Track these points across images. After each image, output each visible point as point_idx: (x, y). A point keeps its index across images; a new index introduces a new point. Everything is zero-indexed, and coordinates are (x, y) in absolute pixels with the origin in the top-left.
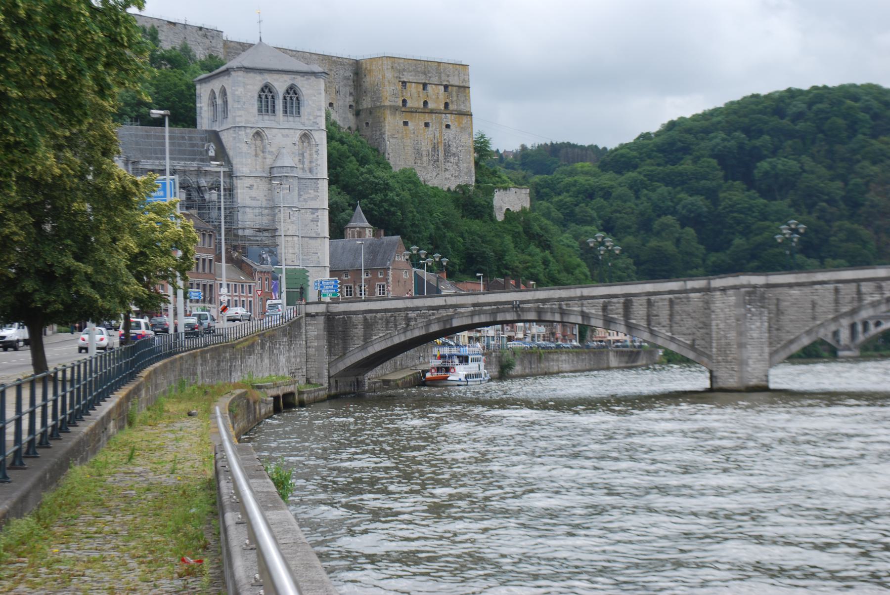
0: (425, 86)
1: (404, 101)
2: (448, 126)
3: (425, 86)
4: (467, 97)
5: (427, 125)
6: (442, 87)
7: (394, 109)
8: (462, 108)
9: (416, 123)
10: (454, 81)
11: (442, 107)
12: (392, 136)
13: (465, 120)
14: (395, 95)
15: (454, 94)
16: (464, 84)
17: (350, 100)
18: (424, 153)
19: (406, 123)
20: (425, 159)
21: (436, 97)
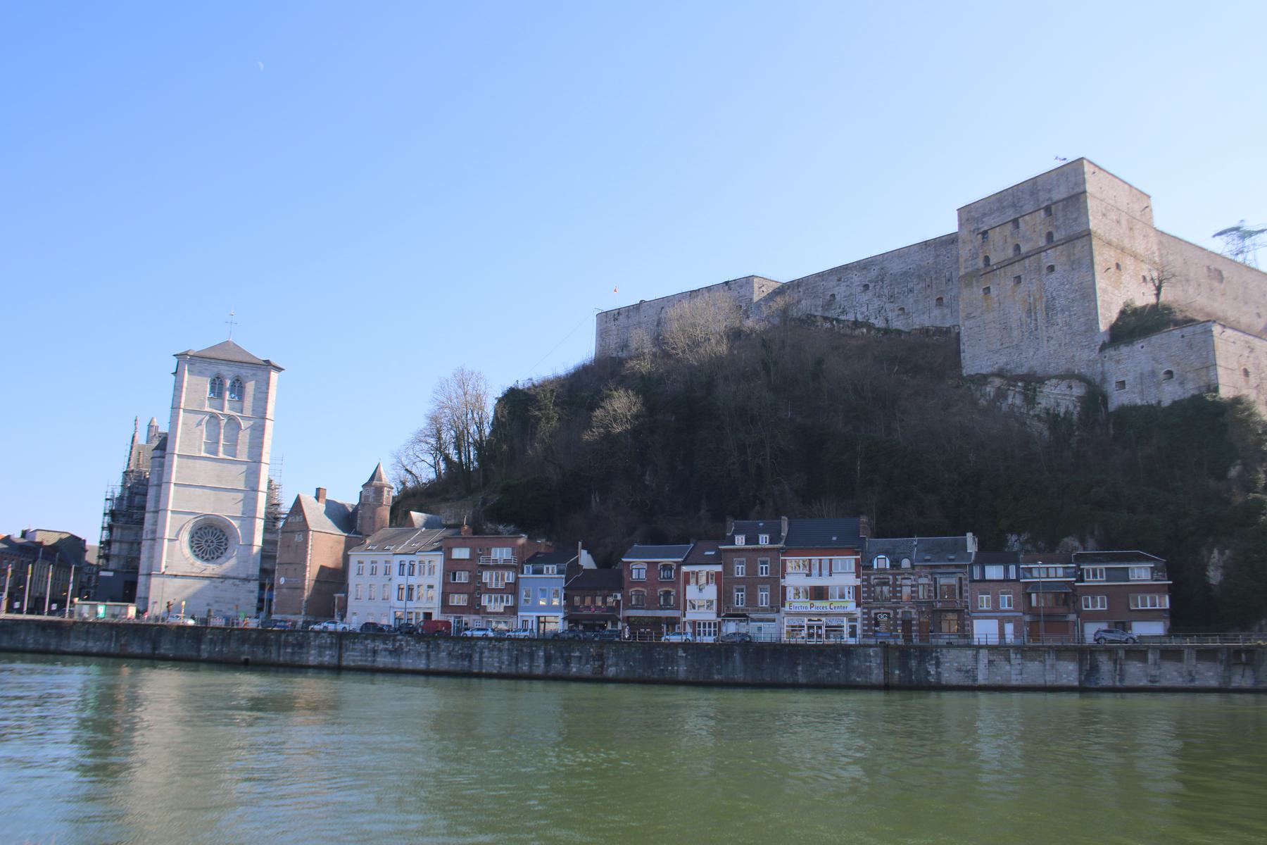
3: (1015, 222)
4: (1084, 210)
5: (1018, 279)
6: (1042, 212)
8: (1077, 229)
9: (1002, 285)
10: (1060, 193)
11: (1042, 242)
13: (1079, 244)
14: (974, 256)
16: (1077, 190)
19: (987, 290)
20: (1015, 333)
21: (1034, 229)
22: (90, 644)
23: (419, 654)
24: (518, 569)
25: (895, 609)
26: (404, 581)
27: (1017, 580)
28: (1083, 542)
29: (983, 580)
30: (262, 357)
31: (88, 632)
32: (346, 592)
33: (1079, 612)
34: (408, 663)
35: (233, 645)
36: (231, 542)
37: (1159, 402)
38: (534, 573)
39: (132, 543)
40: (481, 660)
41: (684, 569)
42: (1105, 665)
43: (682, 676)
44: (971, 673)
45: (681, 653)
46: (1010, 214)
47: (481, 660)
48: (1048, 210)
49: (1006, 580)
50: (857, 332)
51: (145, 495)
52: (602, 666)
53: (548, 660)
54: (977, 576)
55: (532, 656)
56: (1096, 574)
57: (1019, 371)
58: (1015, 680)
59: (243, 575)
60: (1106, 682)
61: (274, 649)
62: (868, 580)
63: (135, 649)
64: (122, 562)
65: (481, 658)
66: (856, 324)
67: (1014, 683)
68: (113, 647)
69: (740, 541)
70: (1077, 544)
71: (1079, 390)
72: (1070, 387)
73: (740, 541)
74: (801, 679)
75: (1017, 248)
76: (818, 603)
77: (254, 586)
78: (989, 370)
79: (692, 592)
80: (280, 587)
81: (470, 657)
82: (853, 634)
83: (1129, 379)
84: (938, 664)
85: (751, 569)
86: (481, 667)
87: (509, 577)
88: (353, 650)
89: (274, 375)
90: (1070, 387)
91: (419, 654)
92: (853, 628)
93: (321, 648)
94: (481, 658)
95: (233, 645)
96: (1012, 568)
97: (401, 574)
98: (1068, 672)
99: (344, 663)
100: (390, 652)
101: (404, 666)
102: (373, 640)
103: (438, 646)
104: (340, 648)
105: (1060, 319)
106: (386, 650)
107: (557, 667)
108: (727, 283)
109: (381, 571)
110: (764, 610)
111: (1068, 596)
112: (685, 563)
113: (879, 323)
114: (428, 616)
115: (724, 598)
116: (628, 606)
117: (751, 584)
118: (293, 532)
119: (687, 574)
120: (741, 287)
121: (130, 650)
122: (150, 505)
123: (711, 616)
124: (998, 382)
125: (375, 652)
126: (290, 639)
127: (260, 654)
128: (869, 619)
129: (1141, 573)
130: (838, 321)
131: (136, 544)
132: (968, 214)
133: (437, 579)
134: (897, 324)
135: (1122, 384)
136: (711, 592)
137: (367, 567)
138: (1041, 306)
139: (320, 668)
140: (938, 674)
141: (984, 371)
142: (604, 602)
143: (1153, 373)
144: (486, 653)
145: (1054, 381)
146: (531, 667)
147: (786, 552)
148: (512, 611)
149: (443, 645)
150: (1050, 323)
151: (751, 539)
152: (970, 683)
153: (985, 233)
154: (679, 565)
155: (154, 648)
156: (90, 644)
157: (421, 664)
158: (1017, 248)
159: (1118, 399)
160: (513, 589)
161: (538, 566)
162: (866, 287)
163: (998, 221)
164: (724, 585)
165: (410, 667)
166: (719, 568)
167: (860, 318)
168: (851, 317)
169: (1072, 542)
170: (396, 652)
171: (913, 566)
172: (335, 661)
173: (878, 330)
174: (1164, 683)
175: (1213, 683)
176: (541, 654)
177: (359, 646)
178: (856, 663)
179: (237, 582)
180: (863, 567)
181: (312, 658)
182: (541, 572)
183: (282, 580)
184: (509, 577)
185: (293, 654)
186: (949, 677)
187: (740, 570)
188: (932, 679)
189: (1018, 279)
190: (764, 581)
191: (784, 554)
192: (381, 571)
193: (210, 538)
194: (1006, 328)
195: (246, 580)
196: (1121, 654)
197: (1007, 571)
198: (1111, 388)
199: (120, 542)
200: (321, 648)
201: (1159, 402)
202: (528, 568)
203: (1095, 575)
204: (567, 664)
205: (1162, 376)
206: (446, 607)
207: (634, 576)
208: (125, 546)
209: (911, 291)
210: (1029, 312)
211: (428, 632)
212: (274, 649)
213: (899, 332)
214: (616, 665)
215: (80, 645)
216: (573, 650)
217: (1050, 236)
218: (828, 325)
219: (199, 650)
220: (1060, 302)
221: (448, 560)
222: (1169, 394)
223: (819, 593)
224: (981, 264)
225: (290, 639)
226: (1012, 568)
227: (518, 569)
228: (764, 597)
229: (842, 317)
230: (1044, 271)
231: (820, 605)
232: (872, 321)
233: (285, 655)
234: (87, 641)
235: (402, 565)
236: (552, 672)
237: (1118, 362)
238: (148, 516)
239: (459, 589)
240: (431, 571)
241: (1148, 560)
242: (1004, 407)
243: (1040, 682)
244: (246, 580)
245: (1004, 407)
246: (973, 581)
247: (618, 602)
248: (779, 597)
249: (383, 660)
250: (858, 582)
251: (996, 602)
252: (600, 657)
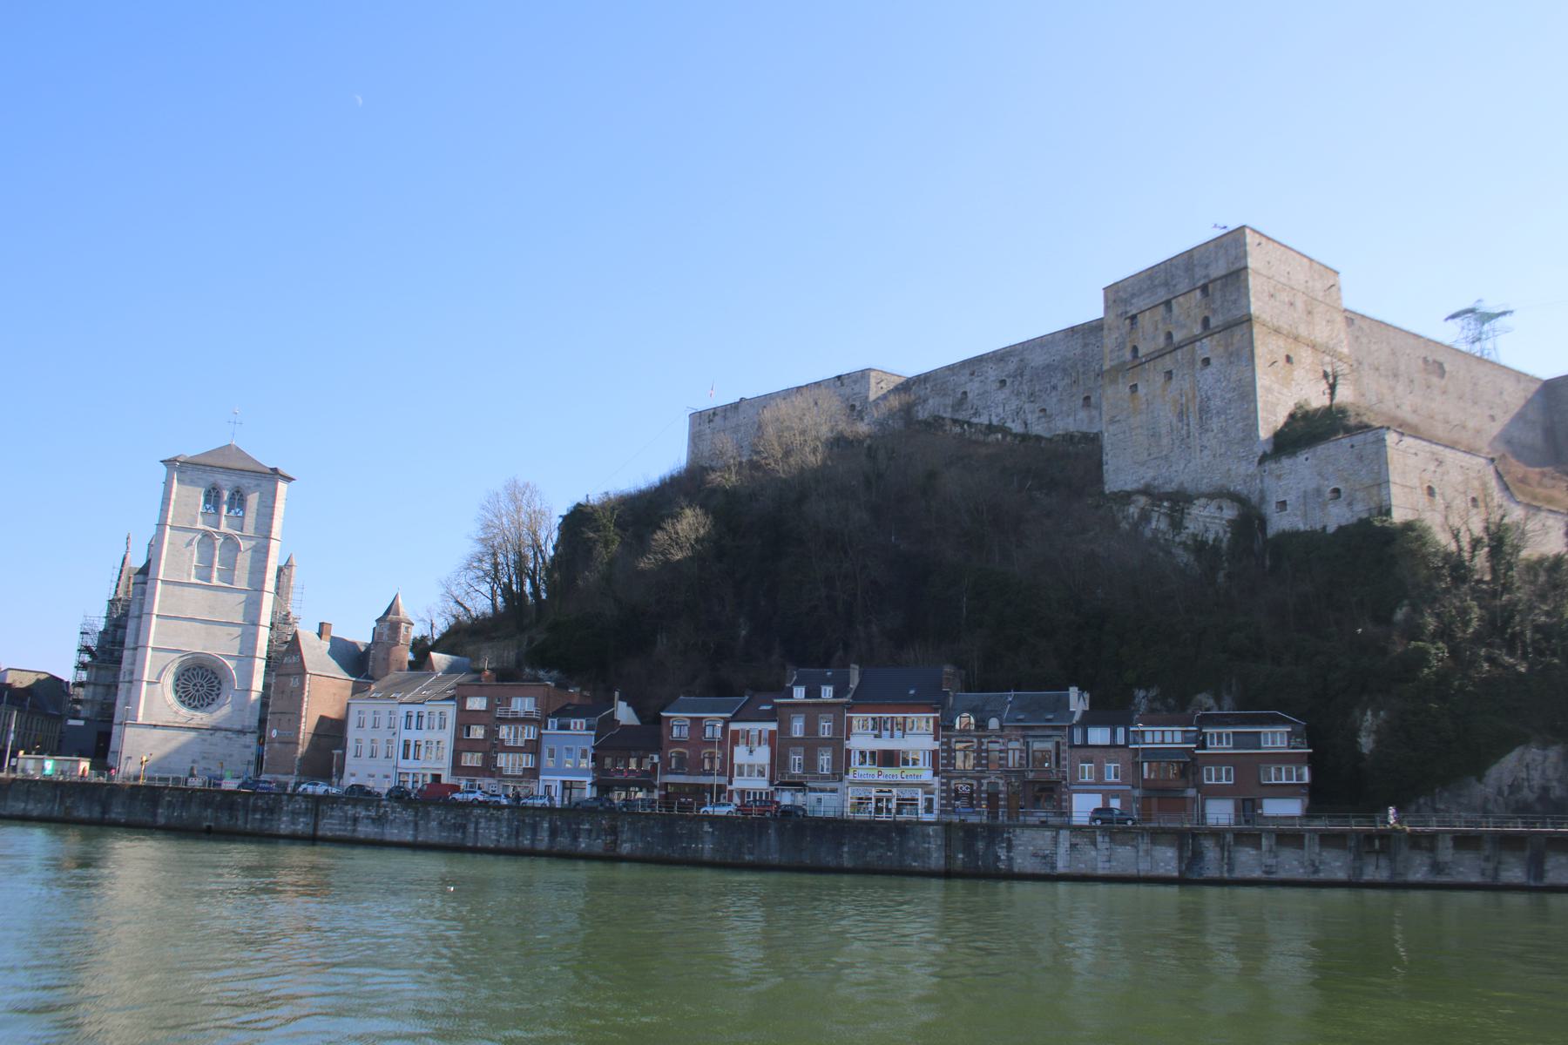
3: (1168, 303)
4: (1243, 290)
5: (1169, 375)
6: (1198, 292)
9: (1151, 383)
10: (1218, 270)
11: (1197, 329)
13: (1238, 333)
14: (1121, 346)
15: (1218, 295)
16: (1237, 266)
18: (1164, 431)
19: (1134, 388)
20: (1165, 441)
22: (30, 807)
23: (406, 823)
24: (541, 723)
25: (979, 779)
27: (1126, 746)
28: (1218, 699)
29: (1085, 745)
30: (270, 464)
31: (28, 793)
32: (344, 749)
33: (1199, 786)
34: (392, 833)
35: (194, 810)
36: (225, 686)
37: (1324, 528)
38: (561, 727)
39: (109, 686)
40: (476, 833)
41: (733, 726)
42: (1211, 852)
43: (707, 856)
44: (1049, 859)
45: (707, 828)
46: (1162, 295)
47: (476, 833)
48: (1204, 289)
49: (1113, 746)
50: (992, 438)
51: (125, 628)
52: (615, 842)
53: (553, 833)
54: (1078, 740)
55: (534, 828)
56: (1220, 740)
57: (1168, 488)
58: (1102, 869)
59: (238, 727)
60: (1212, 872)
61: (241, 815)
62: (948, 743)
63: (82, 813)
64: (97, 708)
65: (476, 829)
66: (991, 428)
67: (1100, 872)
68: (57, 810)
69: (799, 693)
70: (1211, 702)
71: (1230, 512)
72: (1220, 508)
73: (799, 693)
74: (847, 862)
75: (1169, 336)
76: (888, 771)
77: (251, 740)
78: (1135, 486)
79: (740, 755)
80: (272, 741)
81: (463, 827)
82: (929, 809)
83: (1291, 499)
84: (1010, 848)
85: (811, 727)
86: (476, 840)
87: (529, 733)
88: (331, 817)
89: (282, 487)
90: (1220, 508)
91: (406, 823)
92: (930, 801)
93: (295, 814)
94: (476, 829)
95: (194, 810)
96: (1121, 731)
97: (408, 727)
98: (1166, 860)
99: (320, 833)
100: (373, 820)
101: (388, 838)
102: (354, 806)
103: (428, 813)
104: (317, 815)
105: (1215, 424)
106: (368, 817)
107: (563, 842)
108: (839, 377)
109: (384, 724)
110: (825, 778)
111: (1189, 765)
112: (735, 719)
113: (1017, 427)
114: (437, 778)
115: (779, 760)
116: (666, 772)
117: (811, 744)
118: (289, 675)
119: (736, 733)
120: (855, 382)
121: (75, 814)
122: (129, 642)
123: (761, 784)
124: (1143, 500)
125: (355, 820)
126: (260, 803)
127: (225, 821)
128: (948, 791)
129: (1275, 738)
130: (970, 424)
131: (112, 688)
132: (1116, 295)
133: (447, 737)
134: (1038, 429)
135: (1282, 505)
136: (763, 755)
138: (1194, 409)
139: (294, 838)
140: (1010, 859)
141: (1128, 488)
142: (639, 764)
143: (1318, 492)
144: (483, 824)
145: (1203, 501)
146: (533, 841)
147: (851, 708)
148: (533, 773)
149: (434, 812)
150: (1203, 428)
151: (813, 692)
152: (1048, 871)
153: (1133, 318)
154: (727, 722)
155: (104, 813)
156: (30, 807)
157: (408, 836)
158: (1169, 336)
159: (1279, 523)
160: (534, 747)
161: (564, 721)
162: (1003, 382)
164: (780, 746)
165: (395, 839)
166: (773, 726)
167: (995, 421)
168: (984, 420)
169: (1206, 699)
170: (380, 820)
171: (1002, 728)
172: (309, 830)
173: (1016, 435)
174: (1282, 875)
175: (1341, 876)
176: (546, 825)
177: (337, 813)
178: (912, 844)
179: (230, 734)
180: (943, 727)
181: (284, 827)
182: (567, 727)
183: (274, 733)
184: (529, 733)
185: (262, 820)
186: (1023, 863)
187: (798, 727)
188: (1002, 866)
189: (1169, 375)
190: (826, 742)
191: (851, 710)
192: (384, 724)
193: (200, 680)
194: (1155, 435)
195: (242, 732)
196: (1229, 838)
197: (1114, 735)
198: (1270, 510)
199: (95, 685)
200: (295, 814)
201: (1324, 528)
202: (553, 723)
203: (1220, 741)
204: (575, 838)
205: (1328, 495)
206: (457, 768)
207: (675, 732)
208: (100, 690)
209: (1054, 388)
210: (1181, 415)
211: (434, 796)
212: (241, 815)
213: (1038, 438)
214: (632, 840)
215: (19, 807)
216: (582, 822)
217: (1206, 321)
218: (958, 429)
219: (155, 815)
220: (1216, 403)
221: (462, 710)
222: (1336, 517)
223: (888, 759)
224: (1128, 355)
225: (260, 803)
226: (1121, 731)
227: (541, 723)
228: (825, 759)
229: (975, 420)
230: (1199, 364)
231: (890, 773)
232: (1009, 424)
233: (253, 822)
234: (26, 802)
235: (409, 716)
236: (557, 848)
237: (1279, 477)
238: (126, 654)
239: (473, 746)
240: (442, 727)
241: (1284, 722)
242: (1148, 534)
243: (1132, 871)
244: (242, 732)
245: (1148, 534)
246: (1072, 746)
247: (654, 766)
248: (842, 761)
249: (365, 830)
250: (936, 746)
251: (1100, 772)
252: (614, 831)
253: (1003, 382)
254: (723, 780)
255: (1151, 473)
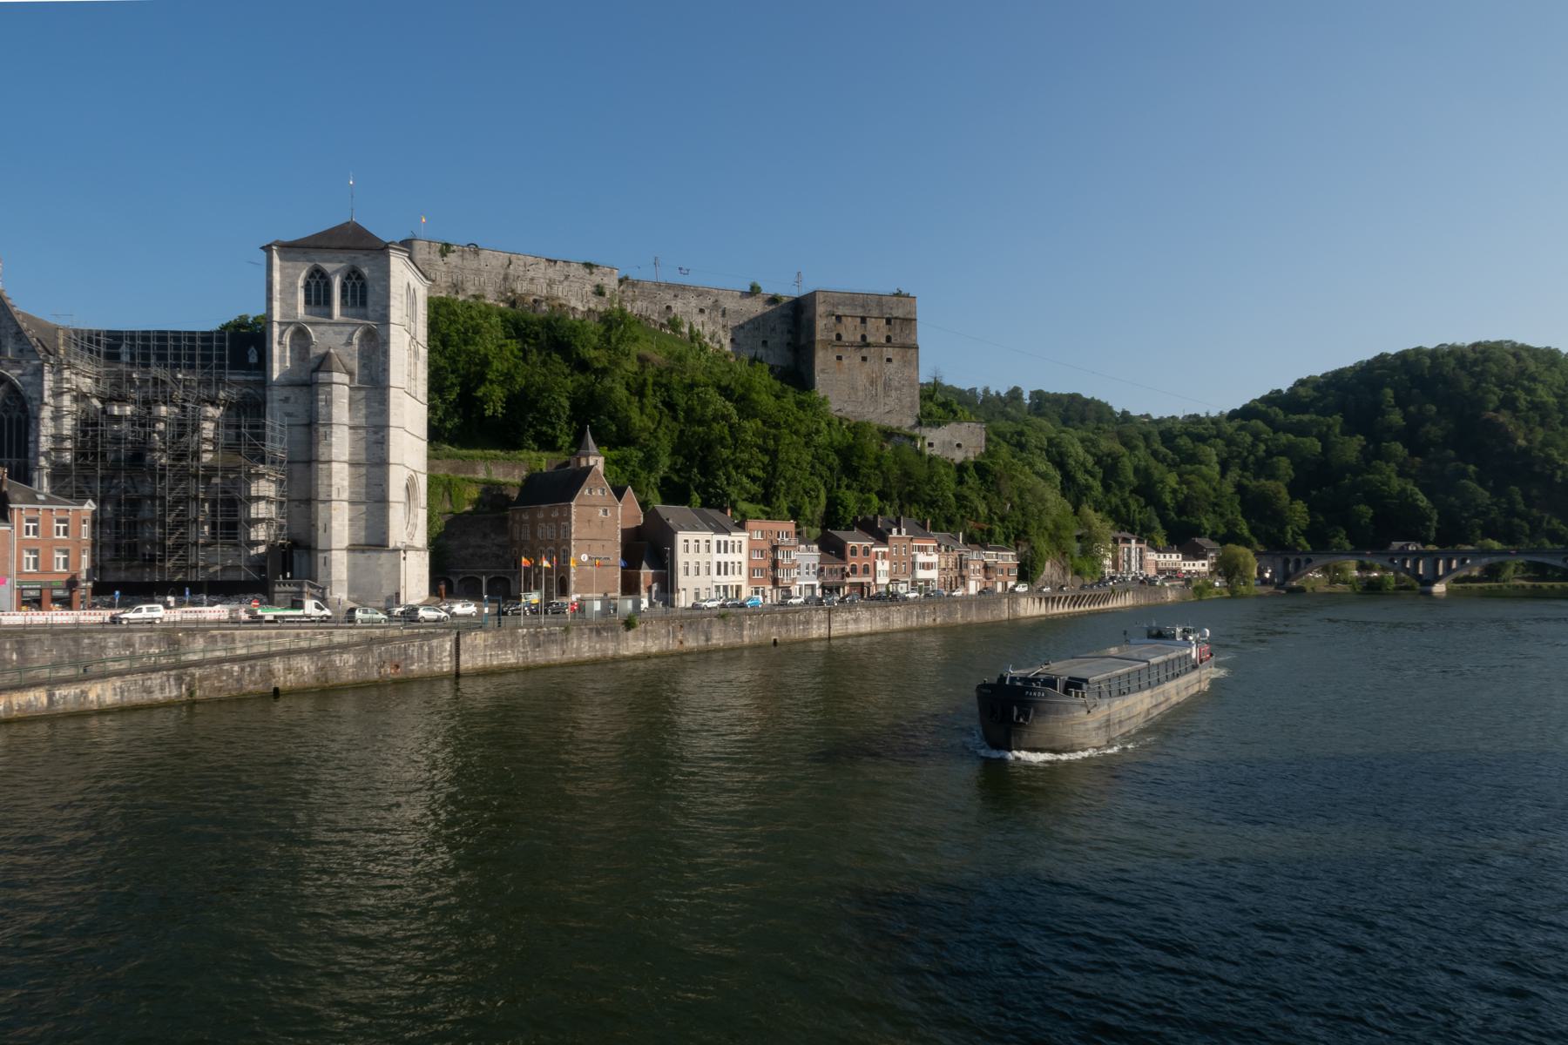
0: (863, 320)
1: (839, 337)
2: (889, 360)
3: (863, 320)
4: (913, 331)
5: (864, 359)
7: (828, 344)
8: (908, 342)
10: (899, 313)
11: (883, 341)
12: (823, 371)
13: (911, 351)
17: (787, 338)
19: (839, 358)
26: (723, 557)
35: (765, 627)
46: (860, 312)
48: (888, 321)
75: (864, 337)
83: (936, 442)
95: (765, 627)
105: (893, 393)
135: (931, 445)
137: (692, 544)
150: (887, 395)
153: (839, 318)
163: (853, 312)
183: (585, 557)
194: (854, 388)
210: (872, 383)
217: (889, 339)
219: (742, 636)
235: (719, 543)
253: (702, 311)
254: (869, 579)
255: (849, 409)
